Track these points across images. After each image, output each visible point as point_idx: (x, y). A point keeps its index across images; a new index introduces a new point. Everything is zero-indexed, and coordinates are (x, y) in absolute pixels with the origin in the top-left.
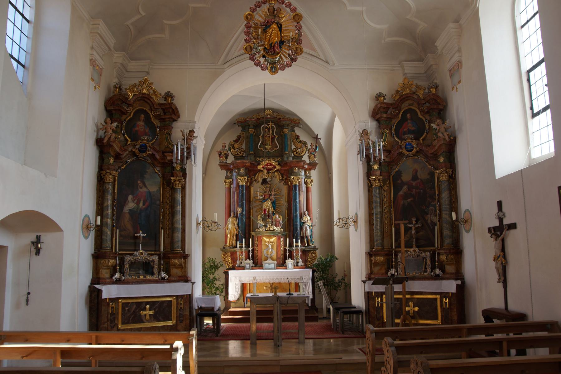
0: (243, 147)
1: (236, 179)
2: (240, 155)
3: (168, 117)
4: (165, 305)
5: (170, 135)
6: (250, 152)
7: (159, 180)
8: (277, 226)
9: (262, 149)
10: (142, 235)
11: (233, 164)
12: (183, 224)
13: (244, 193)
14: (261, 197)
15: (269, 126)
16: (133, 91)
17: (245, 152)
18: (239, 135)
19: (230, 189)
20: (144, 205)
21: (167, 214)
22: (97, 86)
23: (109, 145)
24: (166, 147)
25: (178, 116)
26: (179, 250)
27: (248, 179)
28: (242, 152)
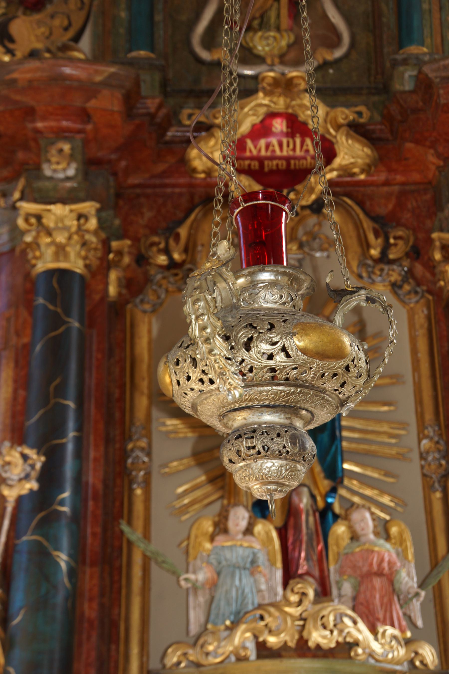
13: (74, 337)
27: (115, 244)
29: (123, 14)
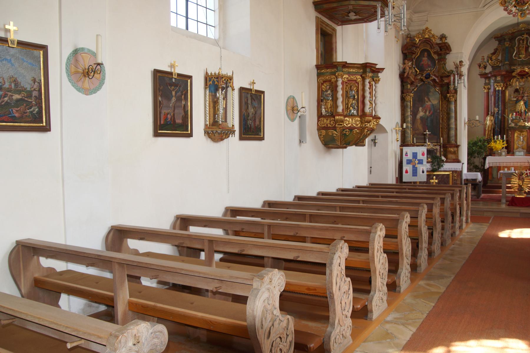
0: (500, 58)
1: (494, 86)
2: (497, 65)
3: (443, 52)
4: (445, 176)
5: (445, 64)
6: (506, 63)
7: (438, 96)
8: (528, 123)
9: (516, 58)
11: (491, 73)
12: (456, 125)
14: (515, 99)
15: (524, 37)
16: (419, 38)
17: (501, 62)
18: (495, 47)
19: (488, 93)
20: (429, 113)
21: (444, 118)
22: (398, 40)
23: (408, 77)
24: (442, 74)
25: (451, 50)
26: (453, 142)
28: (499, 63)
29: (505, 55)
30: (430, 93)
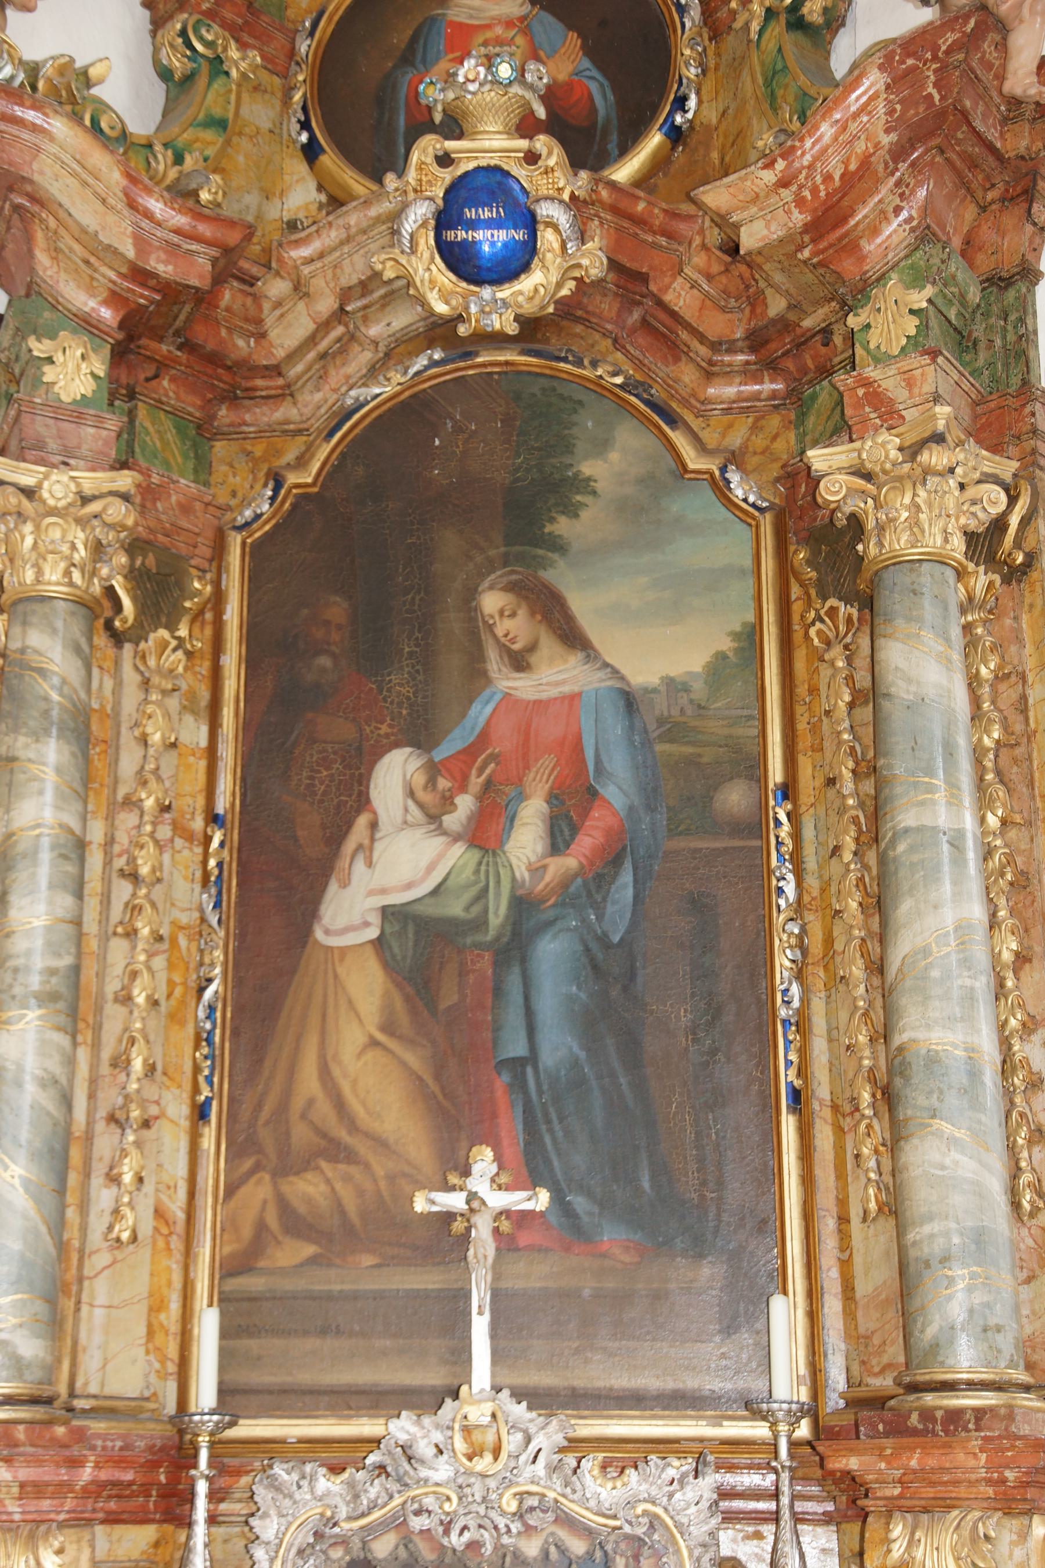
10: (498, 1200)
30: (572, 511)
